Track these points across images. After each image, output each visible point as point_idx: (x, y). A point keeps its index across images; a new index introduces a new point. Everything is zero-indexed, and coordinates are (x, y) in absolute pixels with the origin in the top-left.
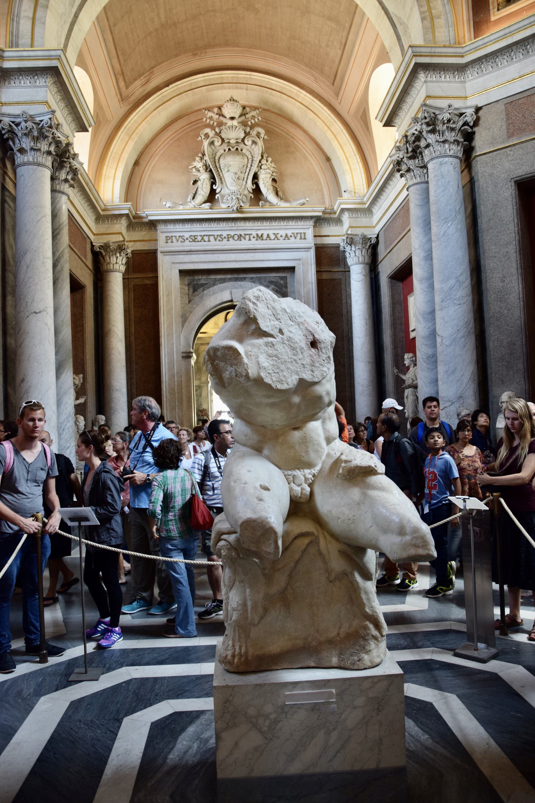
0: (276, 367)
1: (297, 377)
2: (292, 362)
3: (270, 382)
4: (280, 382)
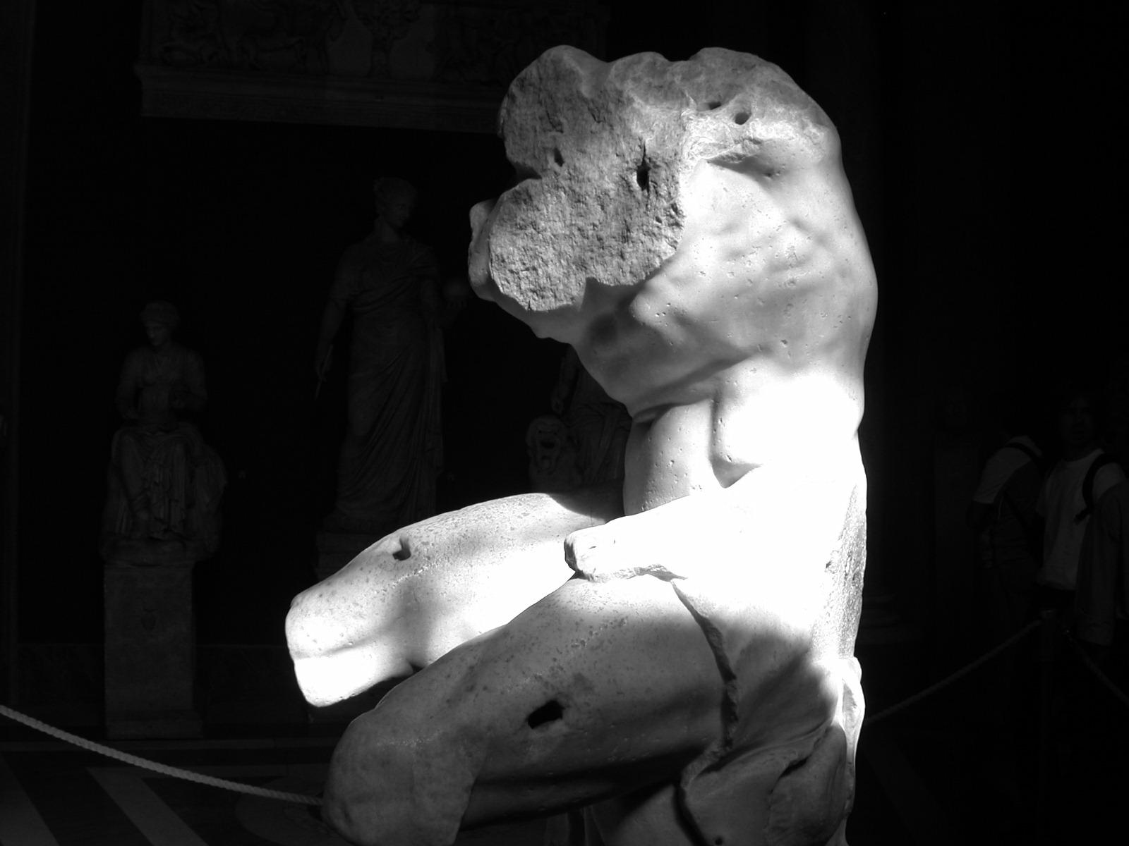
0: (531, 253)
1: (582, 277)
2: (571, 236)
3: (515, 294)
4: (538, 291)
